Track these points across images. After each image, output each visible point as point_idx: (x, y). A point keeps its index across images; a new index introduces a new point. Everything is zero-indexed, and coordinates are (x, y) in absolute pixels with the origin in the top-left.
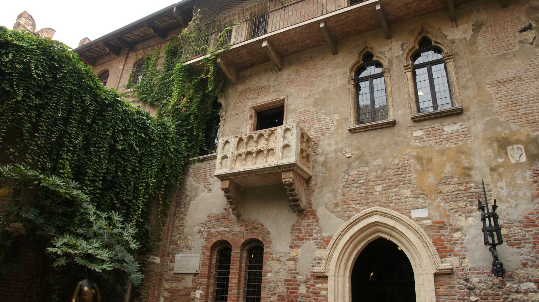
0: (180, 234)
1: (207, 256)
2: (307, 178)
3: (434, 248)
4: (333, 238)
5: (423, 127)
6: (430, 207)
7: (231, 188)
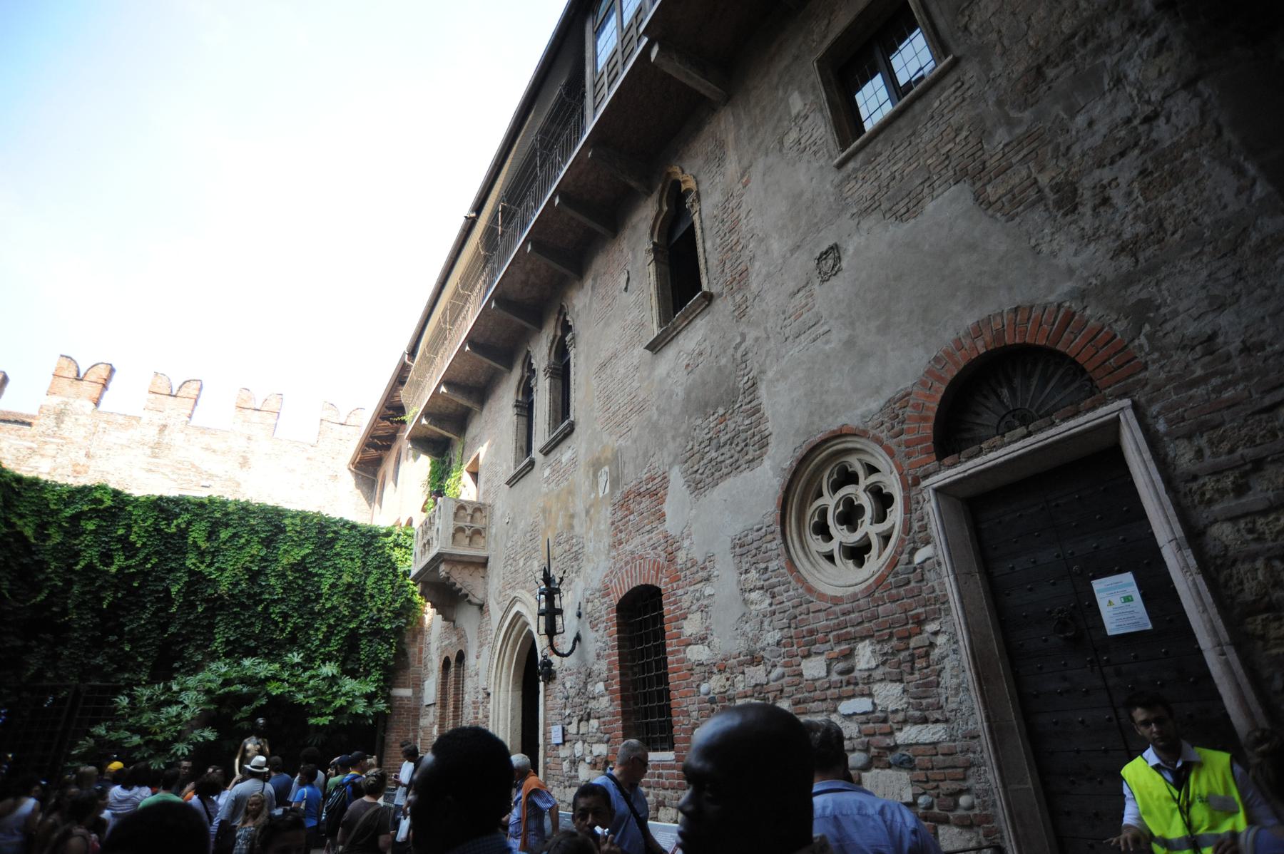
2: (483, 561)
7: (426, 591)
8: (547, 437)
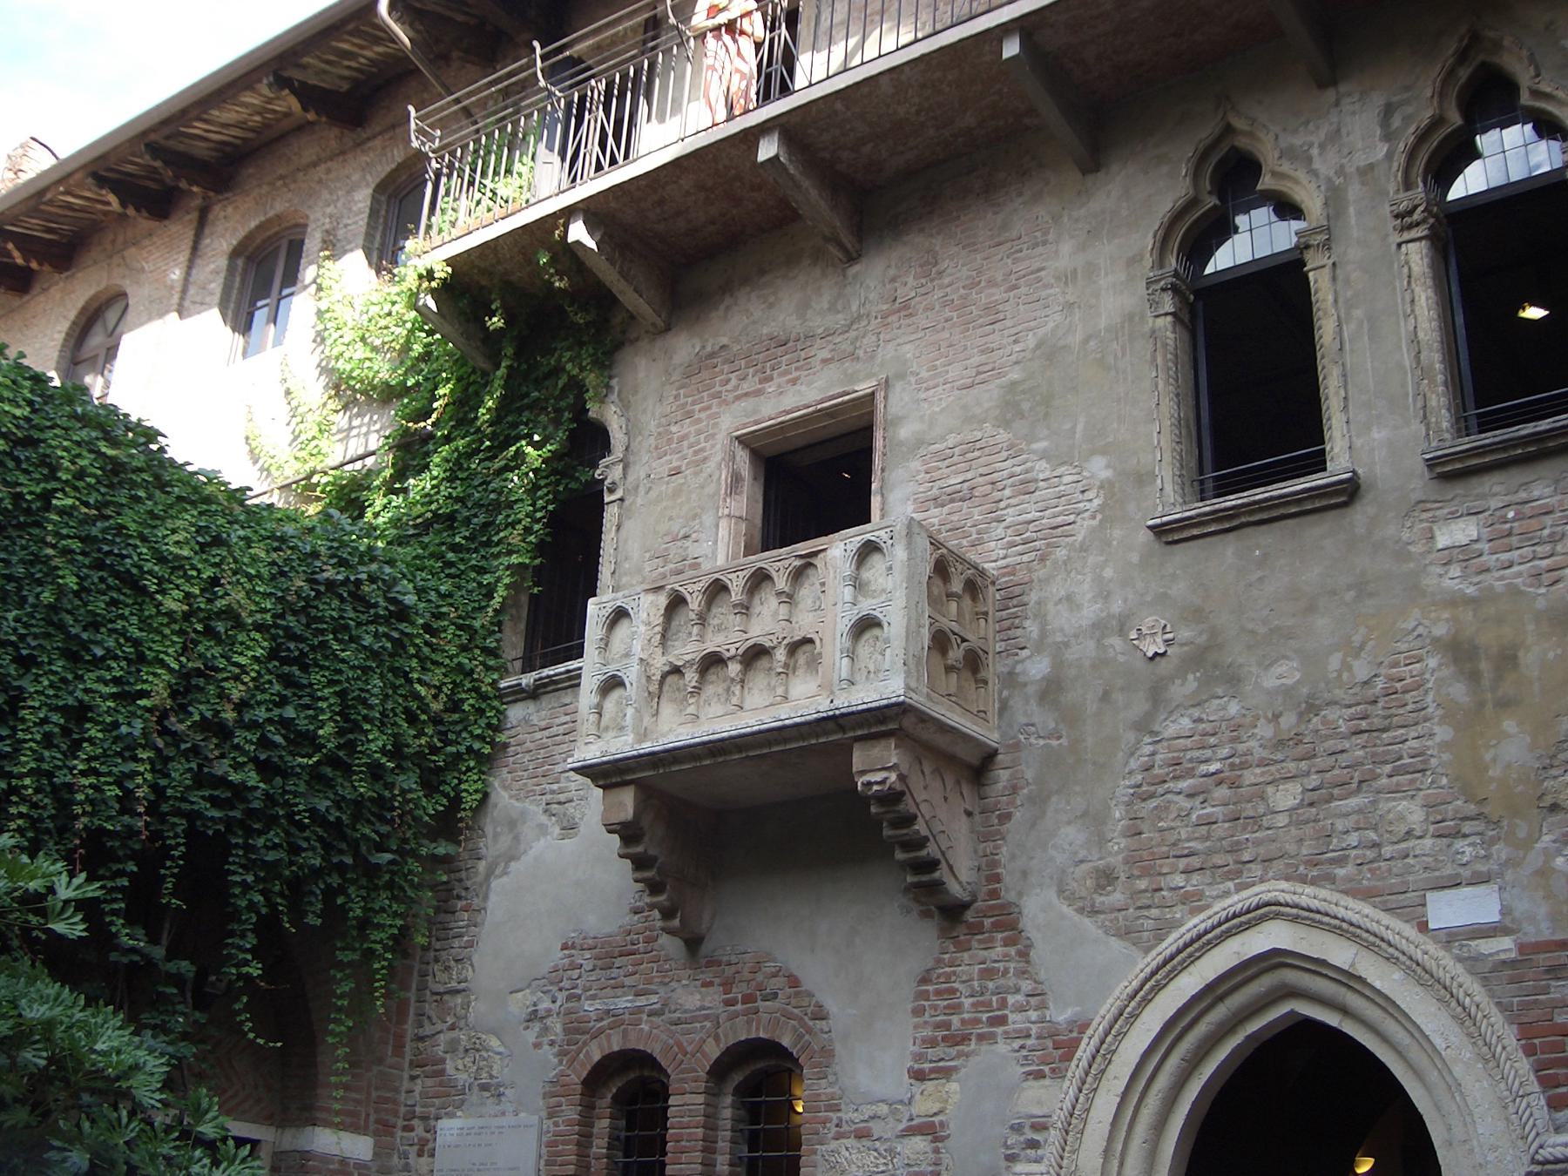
0: (452, 1028)
1: (569, 1123)
2: (973, 758)
3: (1524, 1065)
4: (1090, 1032)
5: (1478, 505)
6: (1509, 875)
7: (646, 822)
8: (1444, 419)
